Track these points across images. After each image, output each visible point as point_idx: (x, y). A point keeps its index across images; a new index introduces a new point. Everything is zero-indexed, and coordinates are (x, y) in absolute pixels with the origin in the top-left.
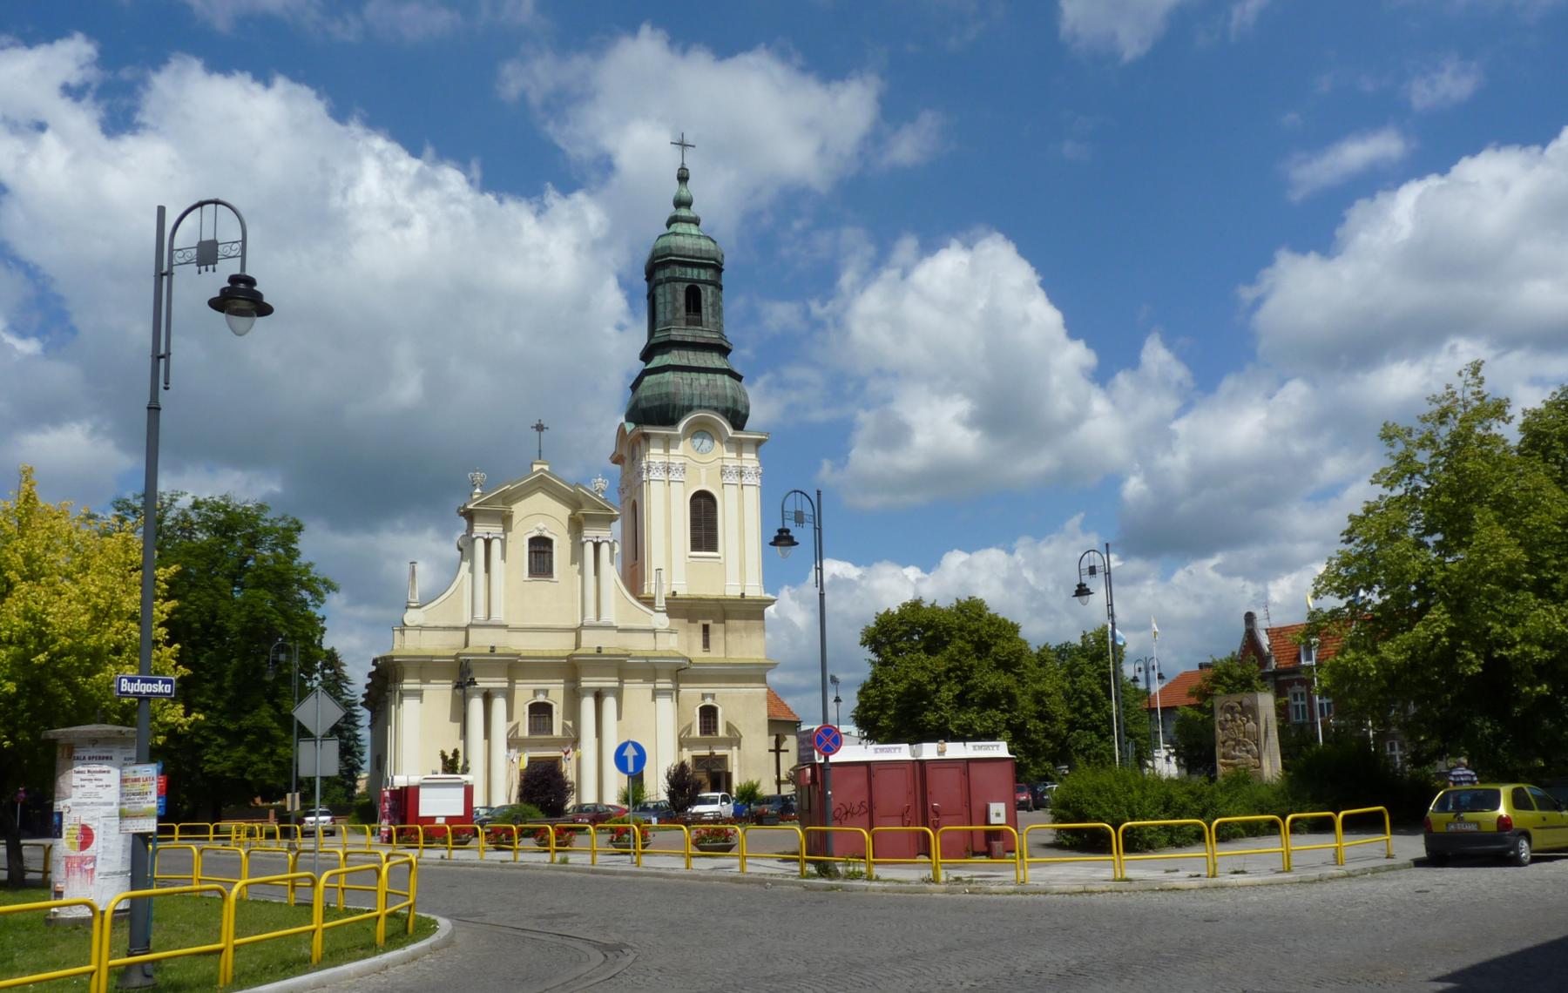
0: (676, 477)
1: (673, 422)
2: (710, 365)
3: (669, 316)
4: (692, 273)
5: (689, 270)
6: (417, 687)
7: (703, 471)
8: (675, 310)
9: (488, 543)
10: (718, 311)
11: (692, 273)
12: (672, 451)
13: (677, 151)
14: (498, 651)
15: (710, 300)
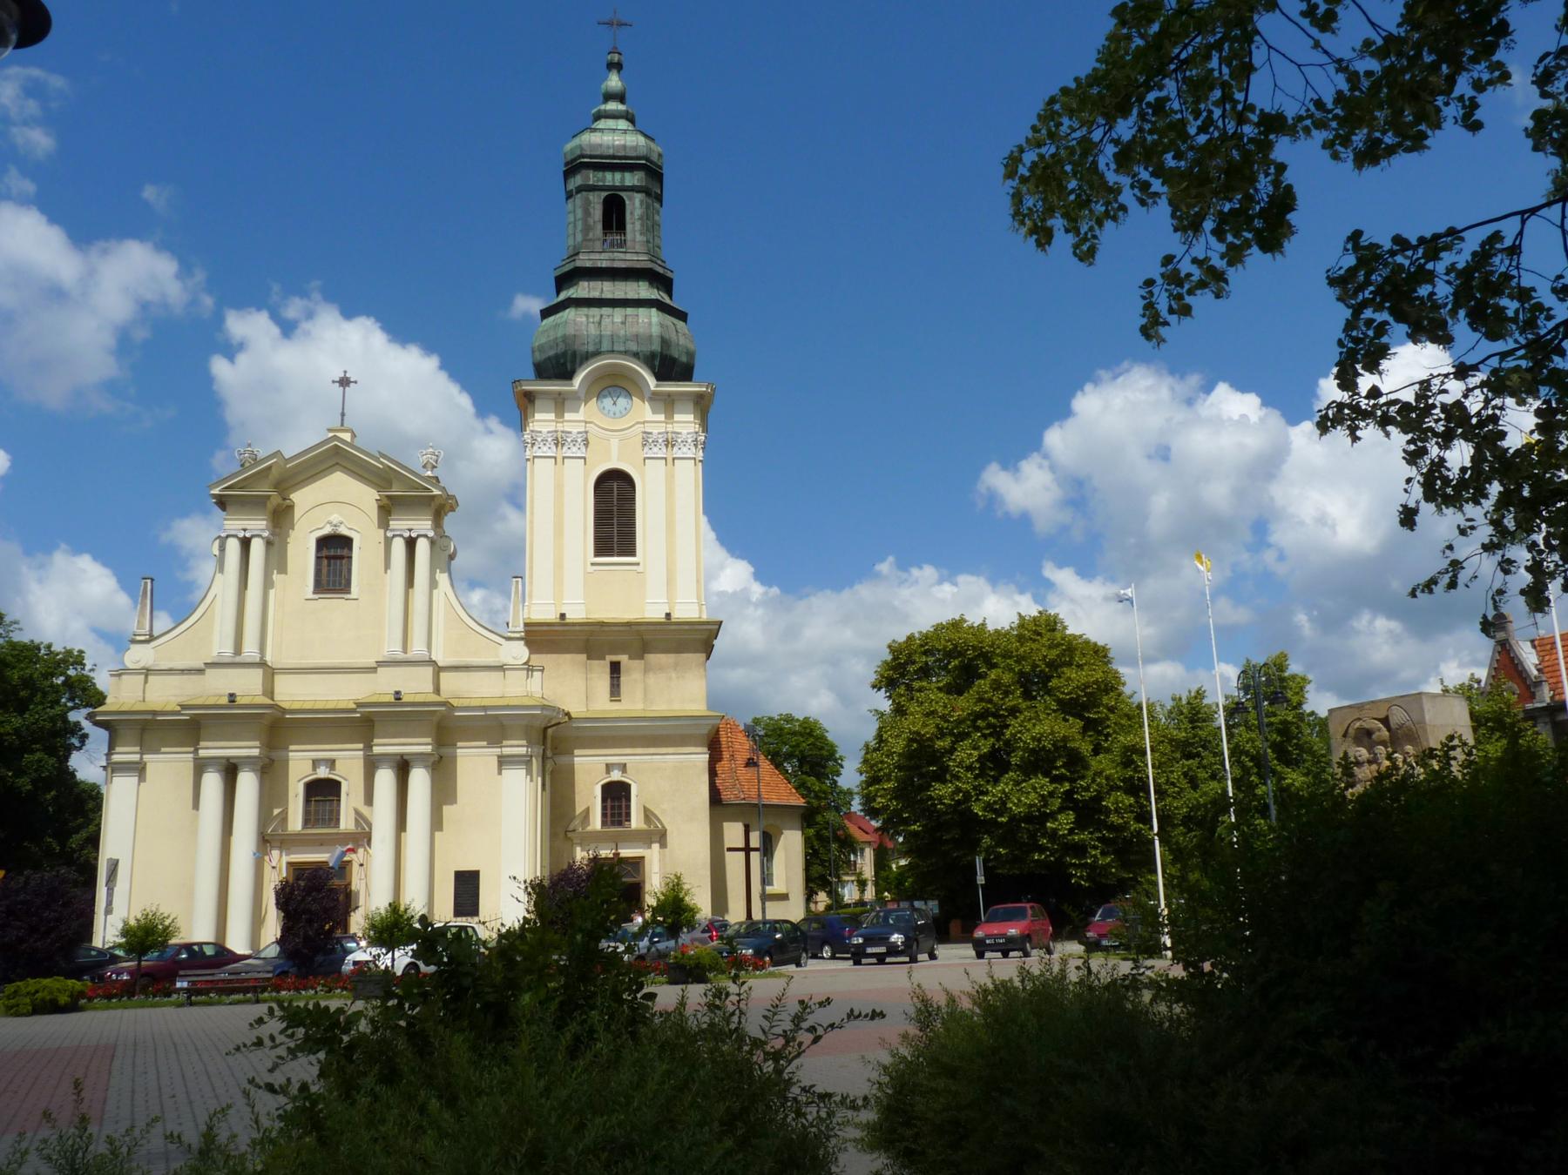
0: (574, 451)
1: (568, 375)
2: (631, 295)
5: (609, 175)
6: (136, 757)
7: (614, 443)
8: (587, 229)
12: (568, 416)
14: (240, 701)
15: (638, 212)
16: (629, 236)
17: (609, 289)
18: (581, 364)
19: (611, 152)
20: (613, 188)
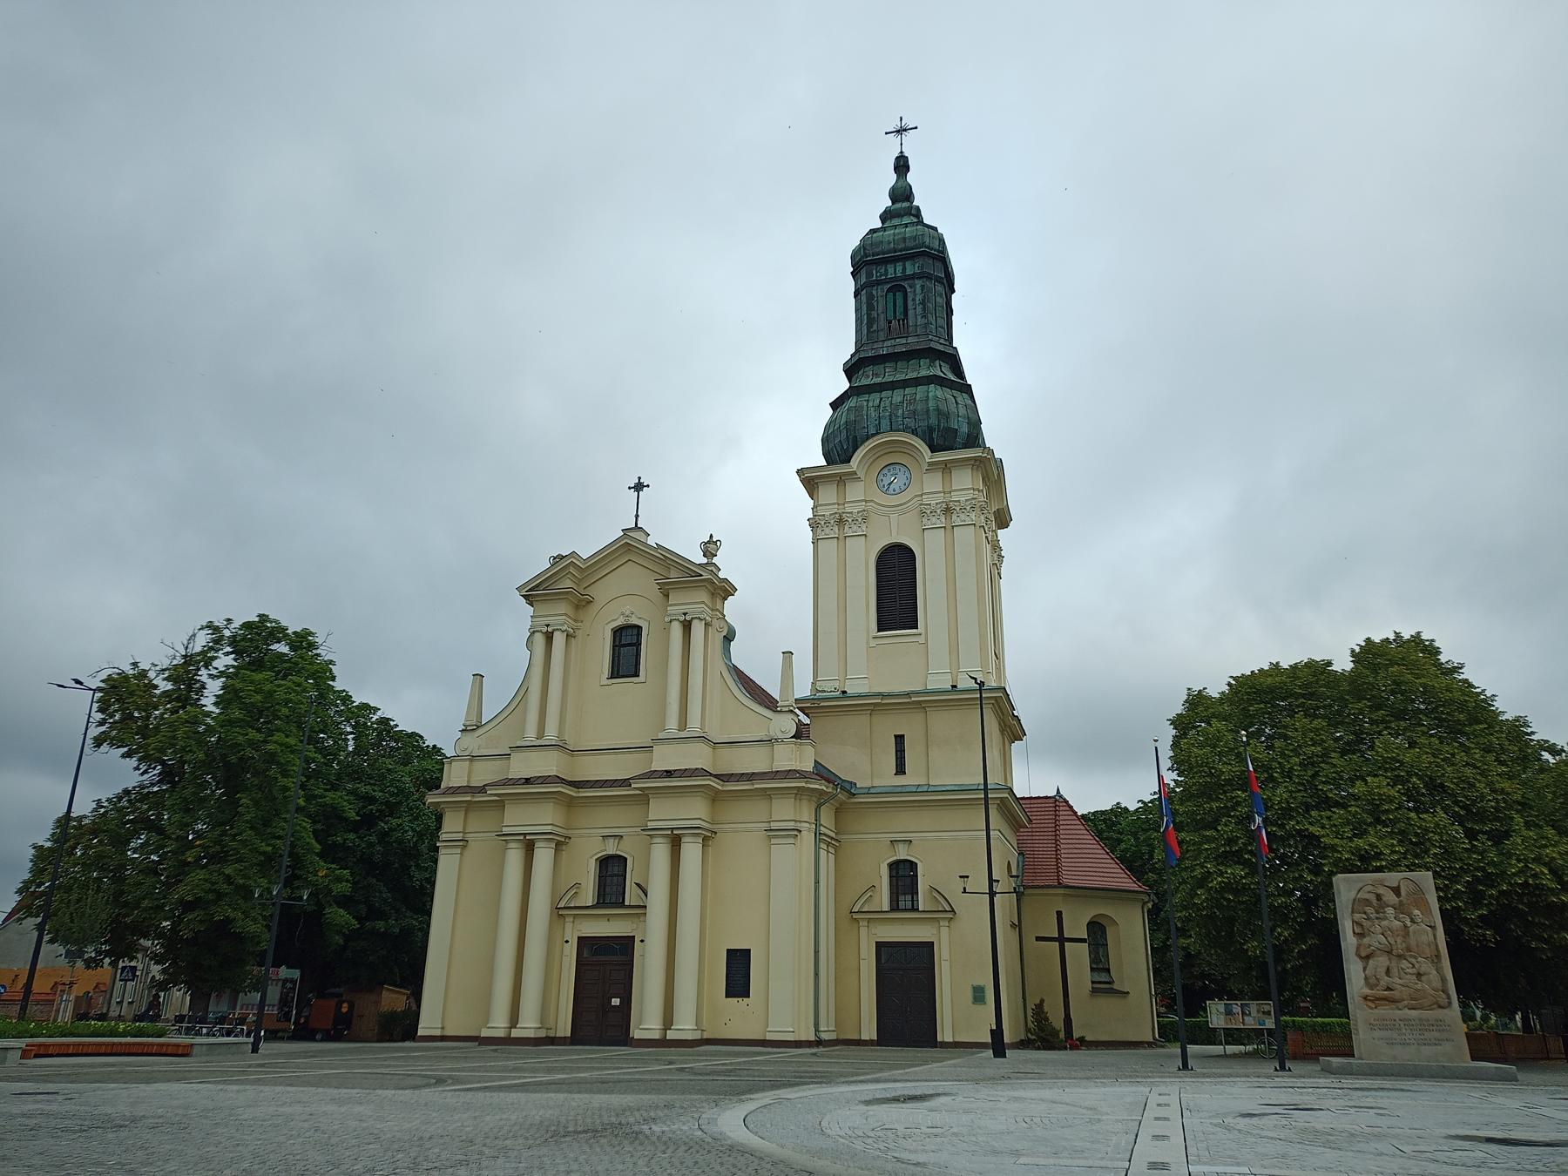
9: (549, 637)
15: (919, 298)
17: (889, 374)
18: (863, 442)
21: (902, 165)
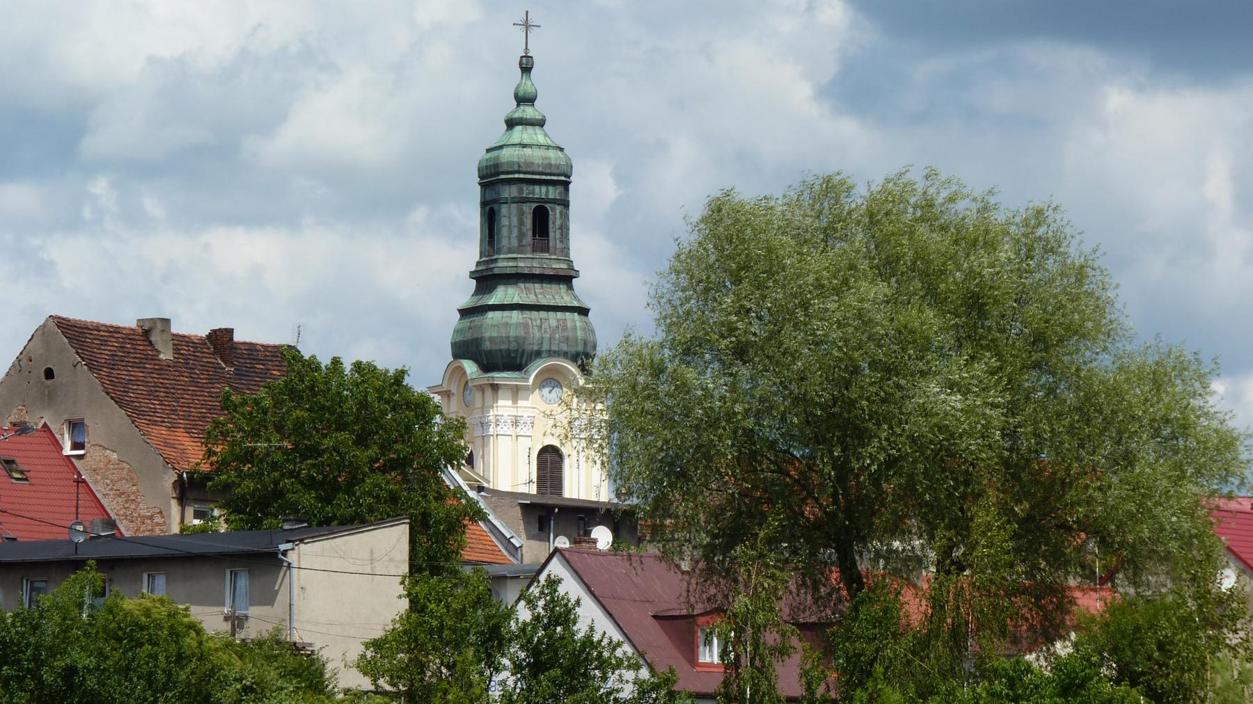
3: (515, 243)
4: (540, 192)
5: (537, 188)
8: (521, 236)
10: (565, 229)
11: (540, 192)
12: (521, 403)
13: (519, 33)
15: (558, 222)
16: (551, 244)
19: (541, 169)
20: (540, 200)
21: (526, 67)
